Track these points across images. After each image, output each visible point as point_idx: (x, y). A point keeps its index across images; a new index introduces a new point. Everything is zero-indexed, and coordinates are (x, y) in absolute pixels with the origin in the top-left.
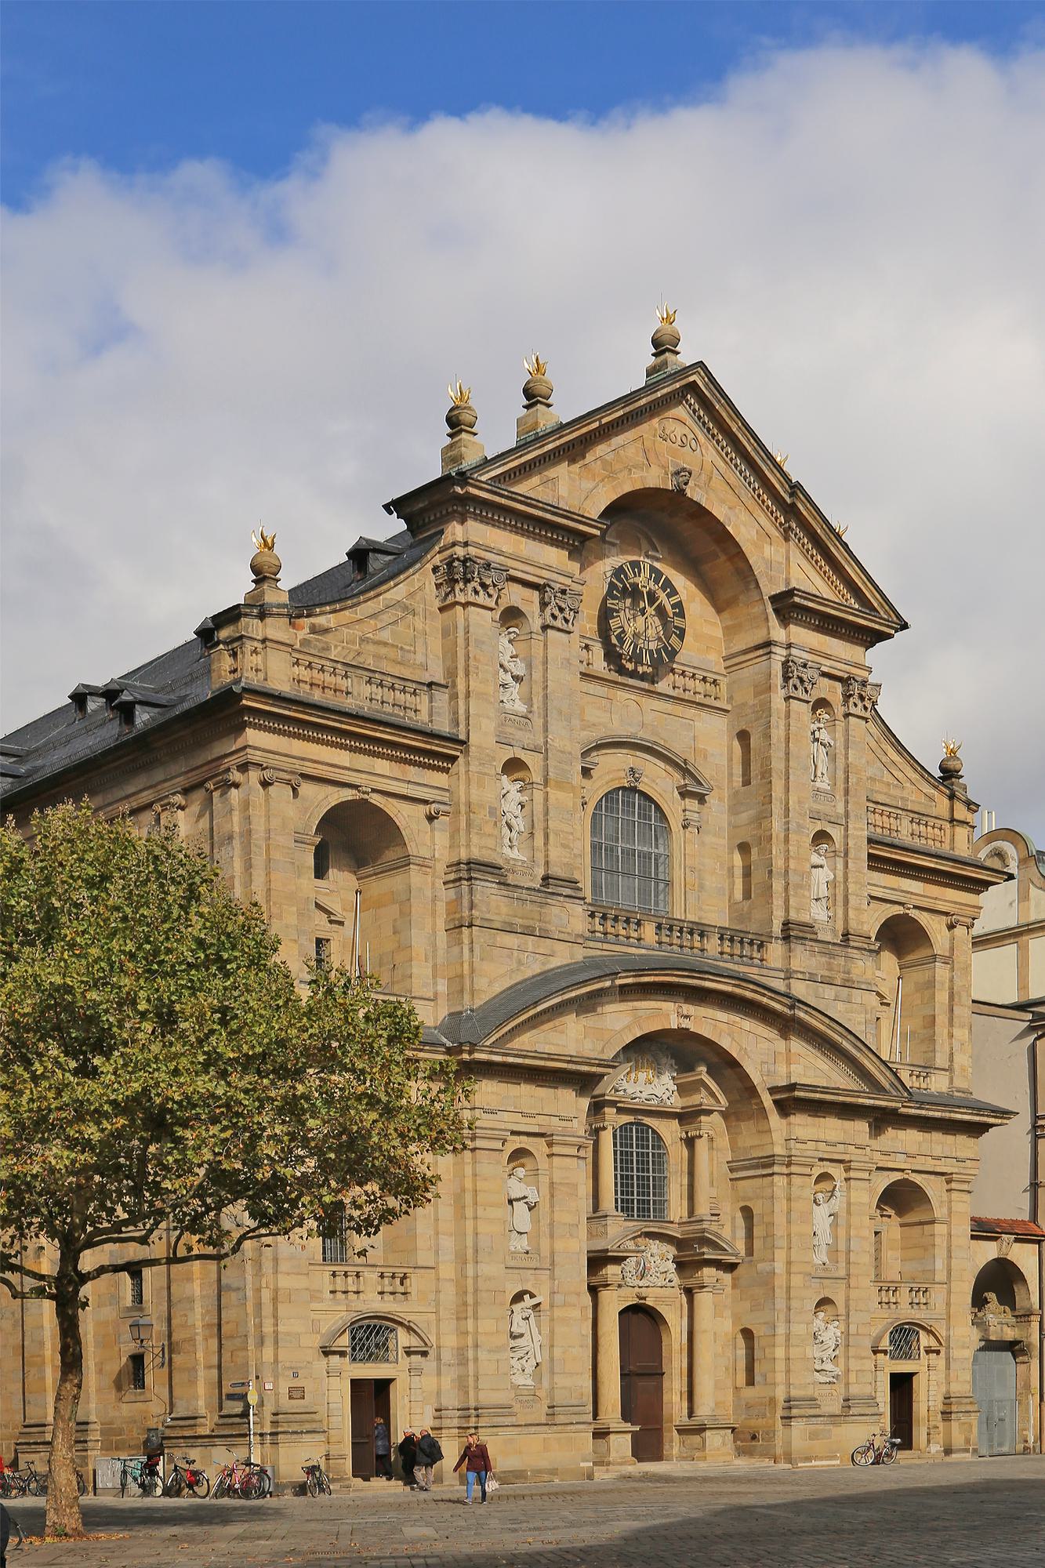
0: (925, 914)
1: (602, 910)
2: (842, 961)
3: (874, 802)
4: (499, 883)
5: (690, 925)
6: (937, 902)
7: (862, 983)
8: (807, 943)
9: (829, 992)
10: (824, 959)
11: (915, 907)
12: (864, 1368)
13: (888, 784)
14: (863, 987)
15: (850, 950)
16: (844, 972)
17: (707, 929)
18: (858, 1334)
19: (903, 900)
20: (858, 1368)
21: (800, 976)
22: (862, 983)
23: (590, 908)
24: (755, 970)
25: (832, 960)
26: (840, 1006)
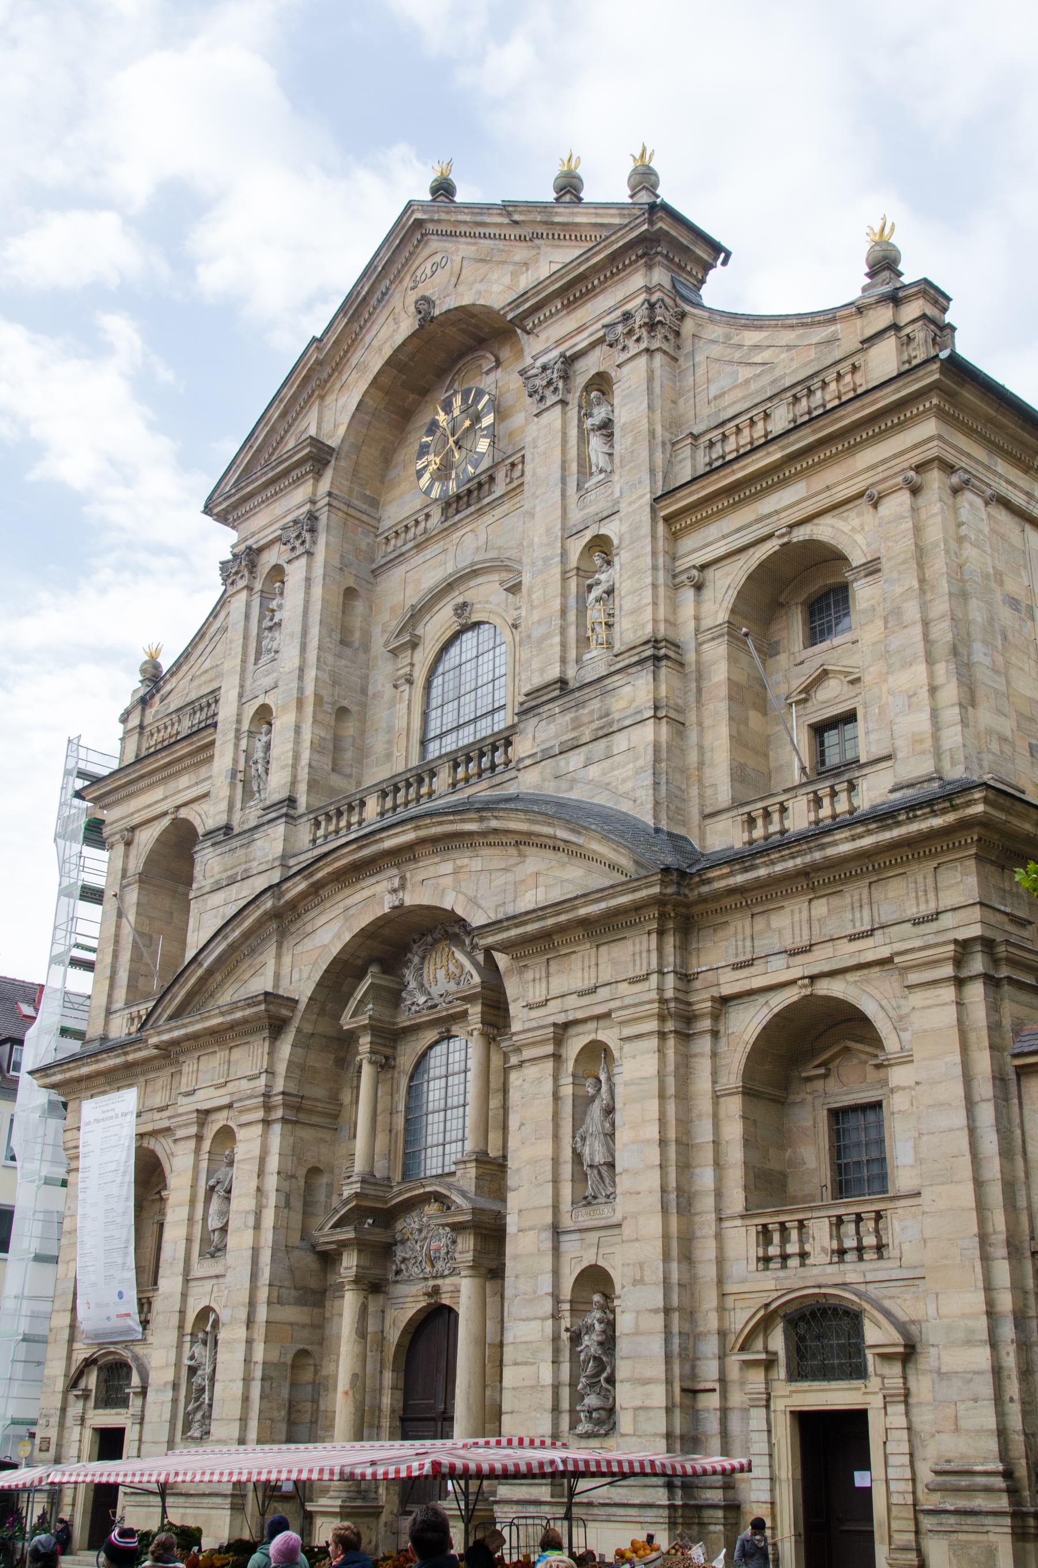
0: (827, 520)
1: (322, 811)
2: (595, 705)
3: (716, 427)
4: (213, 845)
5: (414, 773)
6: (834, 491)
7: (625, 718)
8: (541, 710)
9: (574, 760)
10: (568, 717)
11: (791, 527)
12: (648, 1403)
13: (747, 382)
14: (627, 723)
15: (607, 681)
16: (601, 718)
17: (434, 765)
18: (637, 1333)
19: (765, 531)
20: (639, 1403)
21: (528, 762)
22: (625, 718)
23: (311, 816)
24: (484, 784)
25: (581, 711)
26: (594, 771)
